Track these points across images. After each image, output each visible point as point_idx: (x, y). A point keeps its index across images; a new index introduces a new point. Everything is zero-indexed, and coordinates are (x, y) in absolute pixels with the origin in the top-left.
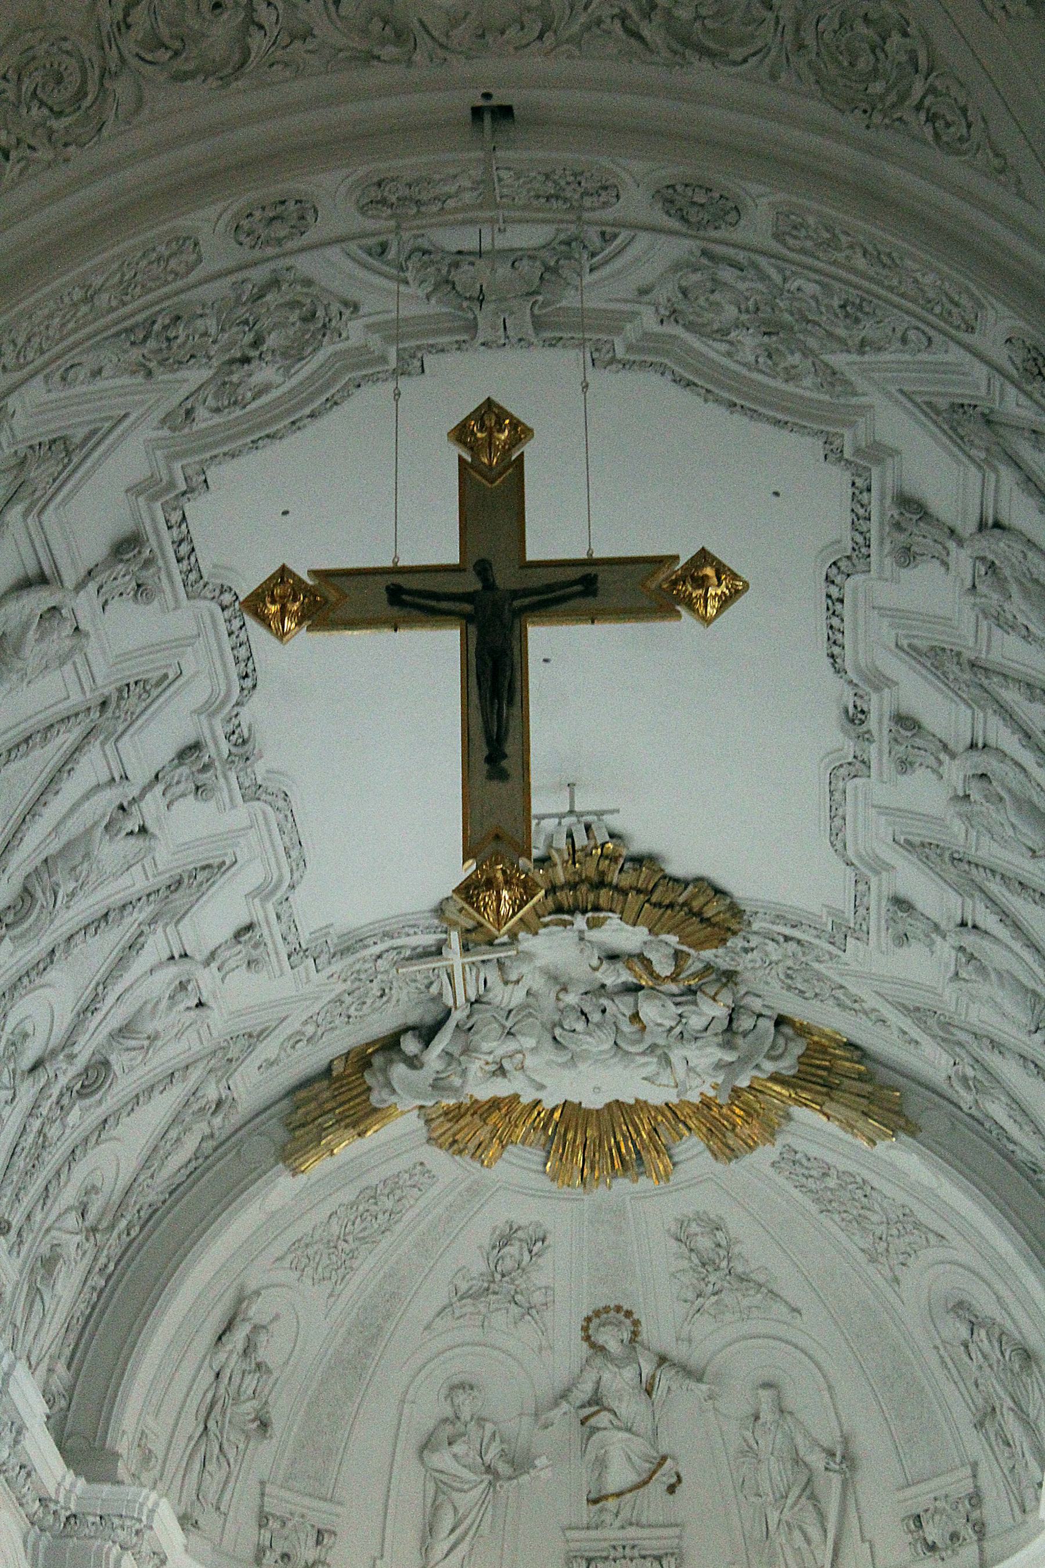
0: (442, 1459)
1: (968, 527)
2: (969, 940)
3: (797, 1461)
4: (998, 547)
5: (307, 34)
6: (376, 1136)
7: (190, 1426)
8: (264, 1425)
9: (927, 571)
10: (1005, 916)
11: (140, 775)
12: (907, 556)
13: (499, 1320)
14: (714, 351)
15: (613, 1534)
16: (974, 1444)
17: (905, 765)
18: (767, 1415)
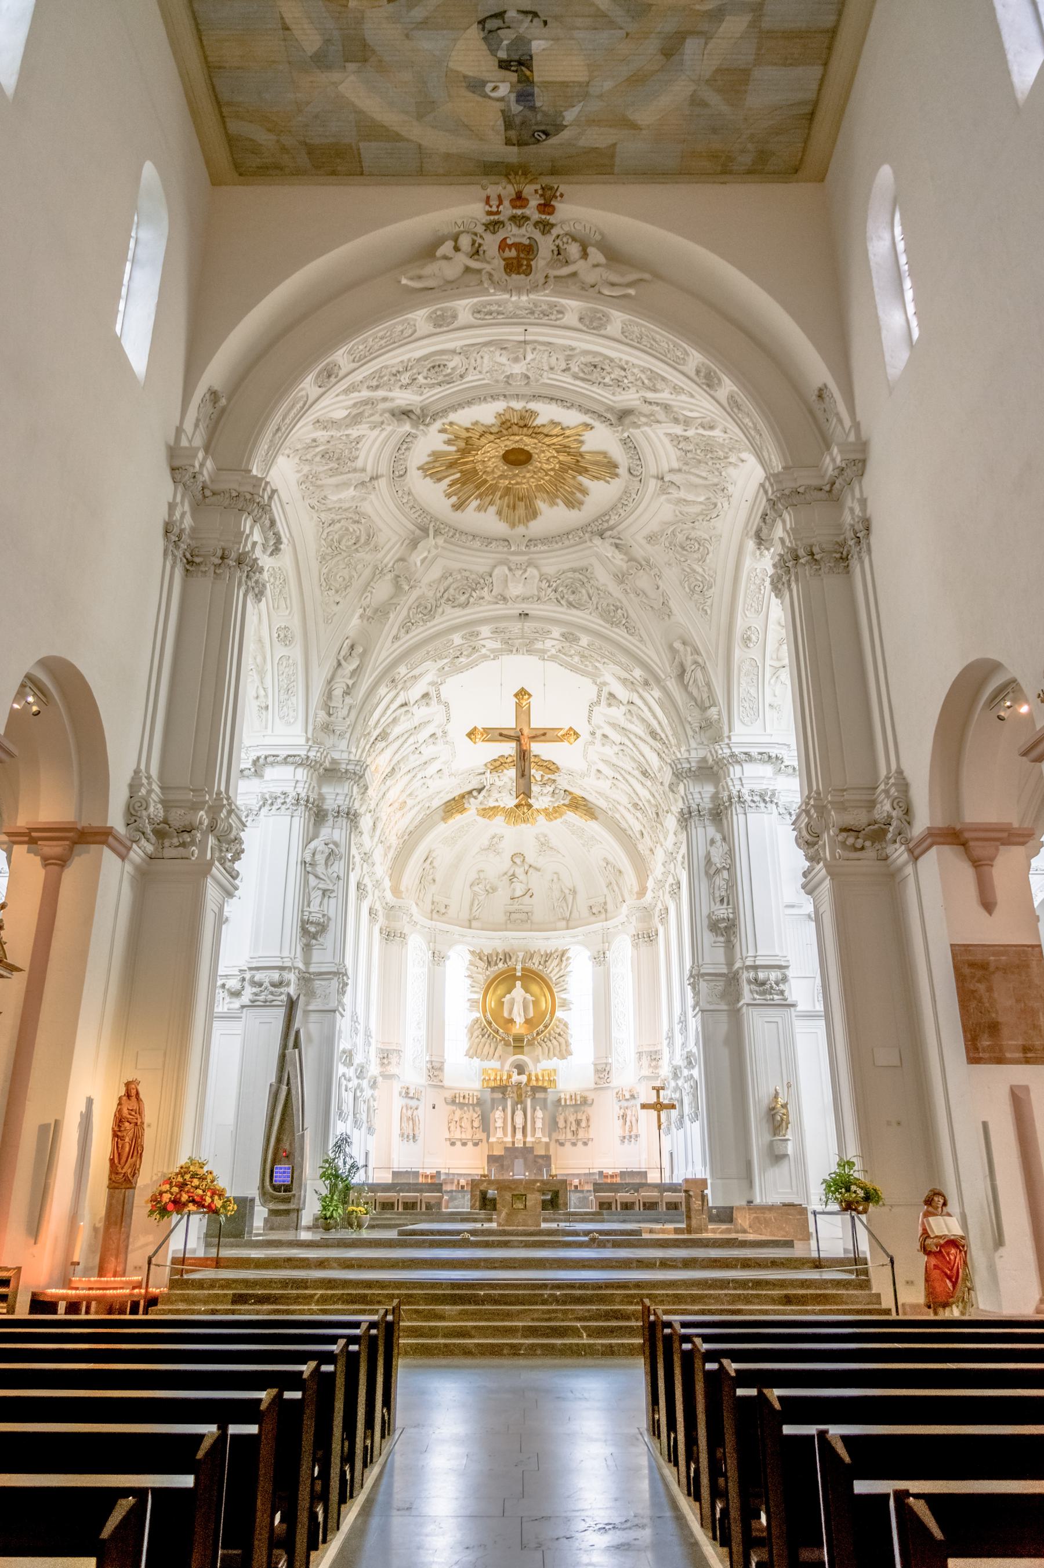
0: (476, 888)
1: (625, 702)
2: (615, 782)
3: (562, 891)
4: (631, 707)
5: (483, 598)
6: (466, 814)
7: (417, 881)
9: (614, 709)
10: (624, 778)
11: (421, 741)
12: (610, 705)
14: (568, 659)
15: (516, 907)
17: (603, 745)
18: (555, 880)
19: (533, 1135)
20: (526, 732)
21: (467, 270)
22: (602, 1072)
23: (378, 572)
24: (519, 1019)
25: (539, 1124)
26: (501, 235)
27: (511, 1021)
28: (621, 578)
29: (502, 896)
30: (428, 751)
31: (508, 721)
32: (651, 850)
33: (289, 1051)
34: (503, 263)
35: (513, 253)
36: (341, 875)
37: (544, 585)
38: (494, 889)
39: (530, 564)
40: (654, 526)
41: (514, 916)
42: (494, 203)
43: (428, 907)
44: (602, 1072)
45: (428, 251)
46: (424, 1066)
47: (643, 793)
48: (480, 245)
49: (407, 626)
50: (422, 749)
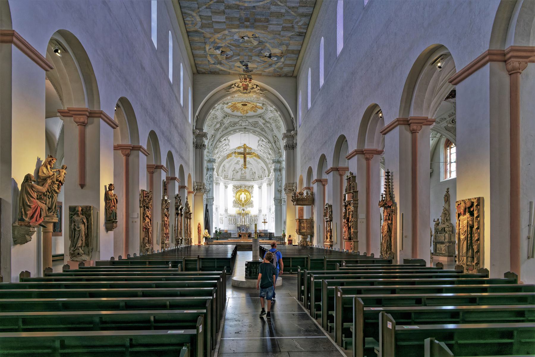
0: (234, 172)
4: (267, 143)
8: (225, 171)
12: (262, 142)
13: (237, 165)
16: (262, 173)
19: (246, 223)
20: (245, 153)
22: (260, 211)
23: (217, 123)
24: (243, 200)
25: (247, 221)
26: (243, 83)
27: (241, 201)
28: (264, 124)
29: (239, 173)
30: (224, 148)
31: (242, 150)
32: (271, 167)
33: (207, 213)
35: (245, 86)
36: (212, 180)
37: (249, 124)
38: (238, 172)
39: (246, 120)
40: (270, 117)
41: (242, 178)
43: (224, 176)
44: (260, 211)
46: (224, 209)
47: (269, 157)
49: (222, 131)
50: (224, 147)
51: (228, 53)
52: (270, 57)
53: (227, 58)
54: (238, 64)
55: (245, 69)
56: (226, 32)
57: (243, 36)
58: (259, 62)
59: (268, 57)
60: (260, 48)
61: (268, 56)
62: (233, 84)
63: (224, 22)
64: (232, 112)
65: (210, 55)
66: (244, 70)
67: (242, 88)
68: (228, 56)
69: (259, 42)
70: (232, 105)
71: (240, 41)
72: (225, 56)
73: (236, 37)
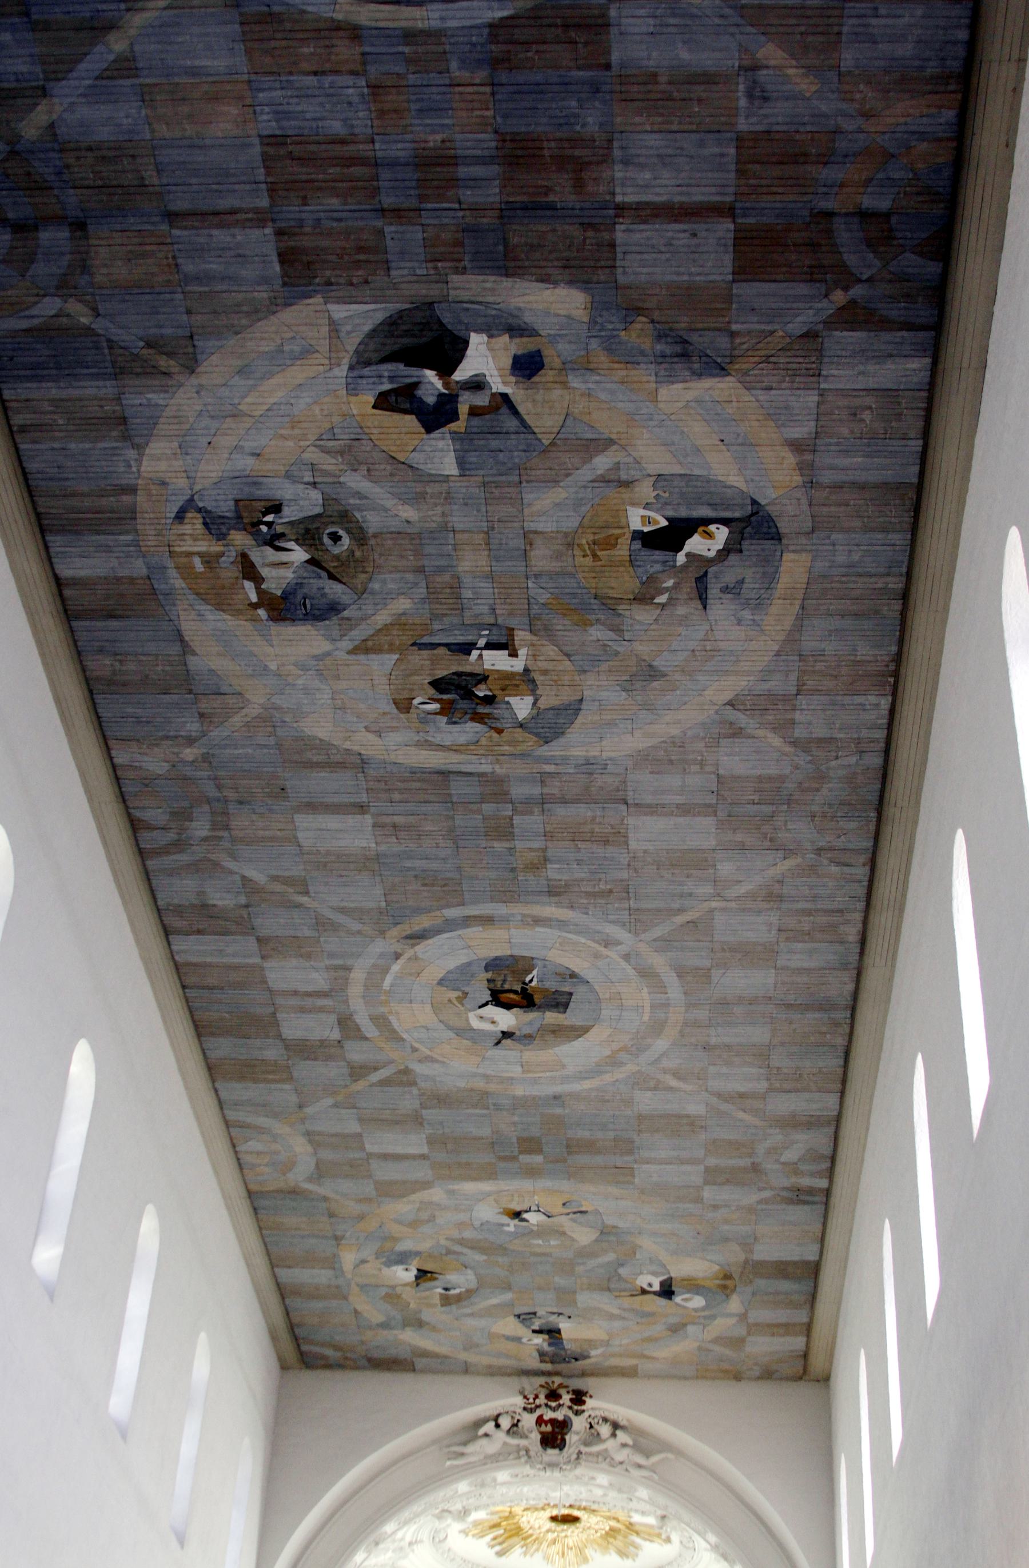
21: (505, 1444)
26: (538, 1412)
34: (539, 1437)
35: (549, 1428)
42: (531, 1397)
45: (473, 1430)
48: (518, 1421)
51: (452, 1278)
52: (667, 1291)
53: (447, 1300)
54: (510, 1326)
55: (546, 1347)
56: (436, 1194)
57: (518, 1209)
58: (612, 1317)
59: (655, 1293)
60: (611, 1257)
61: (656, 1287)
62: (486, 1421)
63: (423, 1157)
64: (500, 1554)
65: (362, 1287)
66: (542, 1355)
67: (536, 1437)
68: (452, 1292)
69: (602, 1233)
70: (495, 1519)
71: (507, 1229)
72: (440, 1290)
73: (487, 1213)
